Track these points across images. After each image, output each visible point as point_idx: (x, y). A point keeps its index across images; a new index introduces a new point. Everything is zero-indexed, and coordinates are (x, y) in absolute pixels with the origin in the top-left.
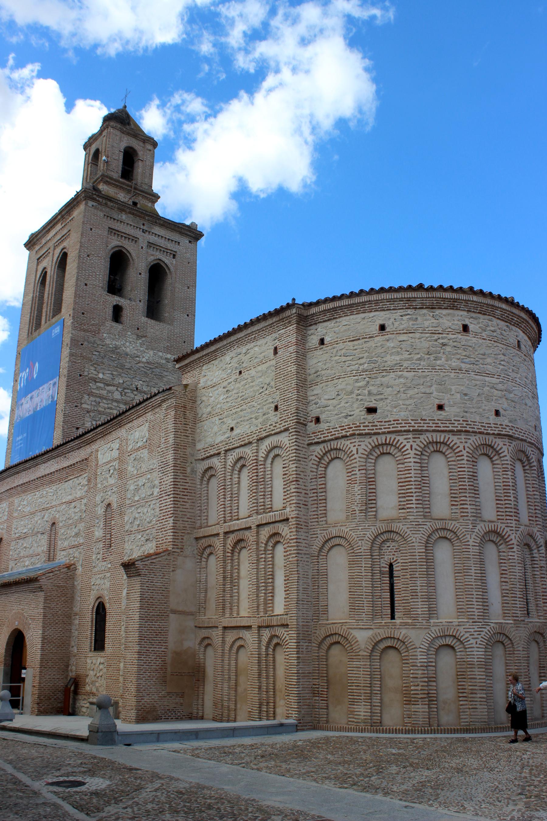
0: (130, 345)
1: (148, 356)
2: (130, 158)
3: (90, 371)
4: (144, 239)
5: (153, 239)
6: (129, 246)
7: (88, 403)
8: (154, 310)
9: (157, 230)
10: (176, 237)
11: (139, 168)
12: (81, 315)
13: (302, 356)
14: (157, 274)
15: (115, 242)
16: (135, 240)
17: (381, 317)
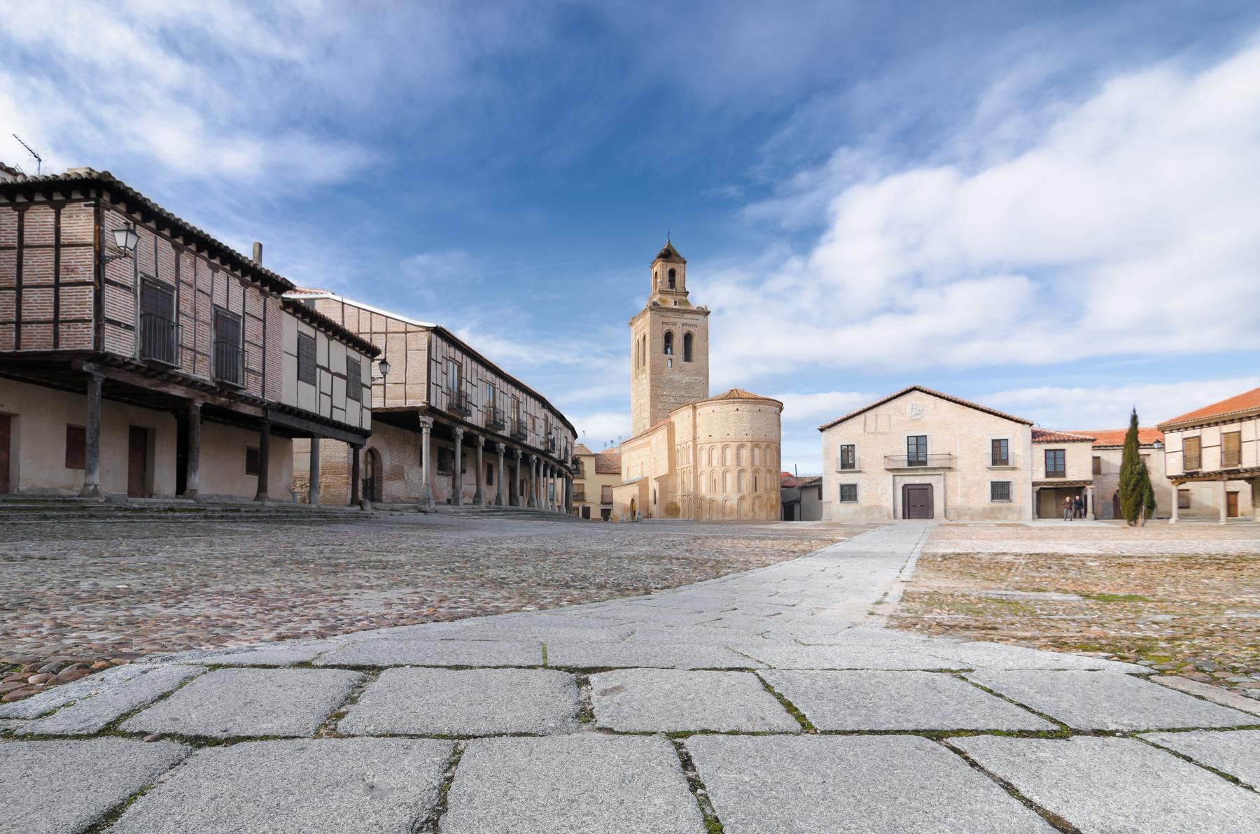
0: (677, 377)
1: (687, 379)
2: (672, 273)
3: (660, 391)
4: (679, 321)
5: (685, 321)
6: (672, 328)
7: (660, 406)
8: (688, 357)
9: (687, 316)
10: (696, 316)
11: (678, 278)
12: (653, 367)
13: (695, 418)
14: (688, 338)
15: (666, 328)
16: (675, 324)
17: (713, 408)
